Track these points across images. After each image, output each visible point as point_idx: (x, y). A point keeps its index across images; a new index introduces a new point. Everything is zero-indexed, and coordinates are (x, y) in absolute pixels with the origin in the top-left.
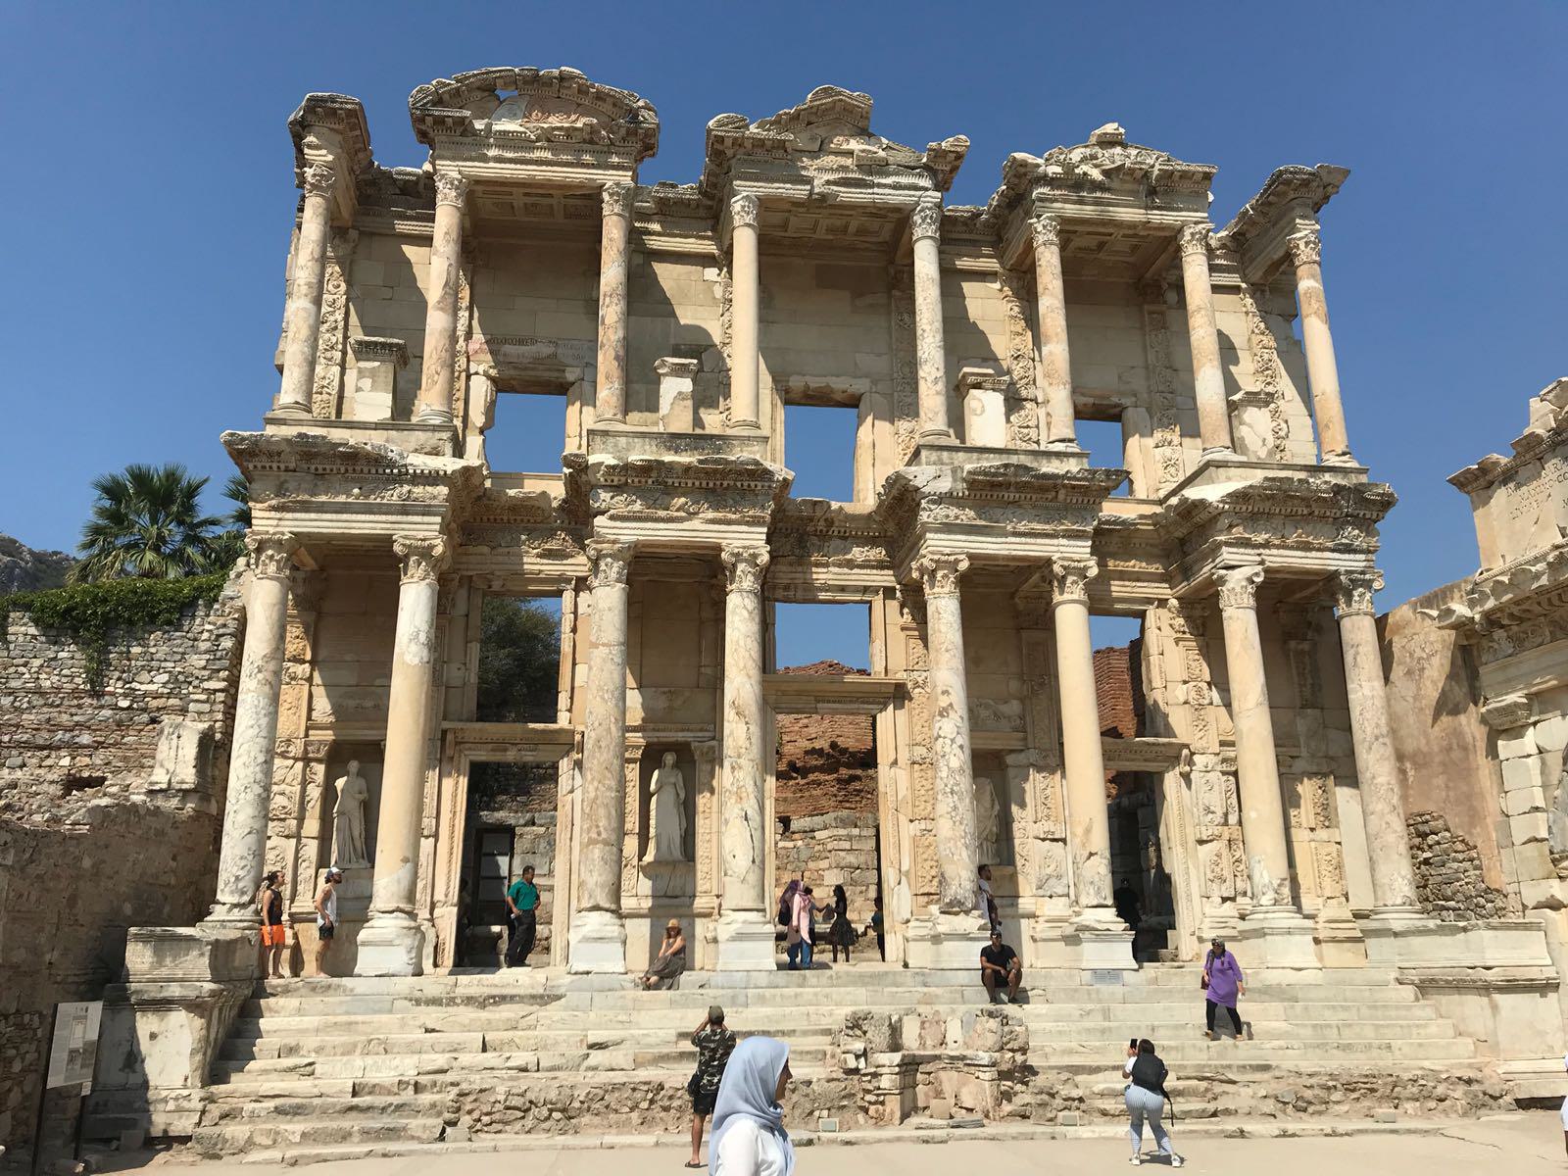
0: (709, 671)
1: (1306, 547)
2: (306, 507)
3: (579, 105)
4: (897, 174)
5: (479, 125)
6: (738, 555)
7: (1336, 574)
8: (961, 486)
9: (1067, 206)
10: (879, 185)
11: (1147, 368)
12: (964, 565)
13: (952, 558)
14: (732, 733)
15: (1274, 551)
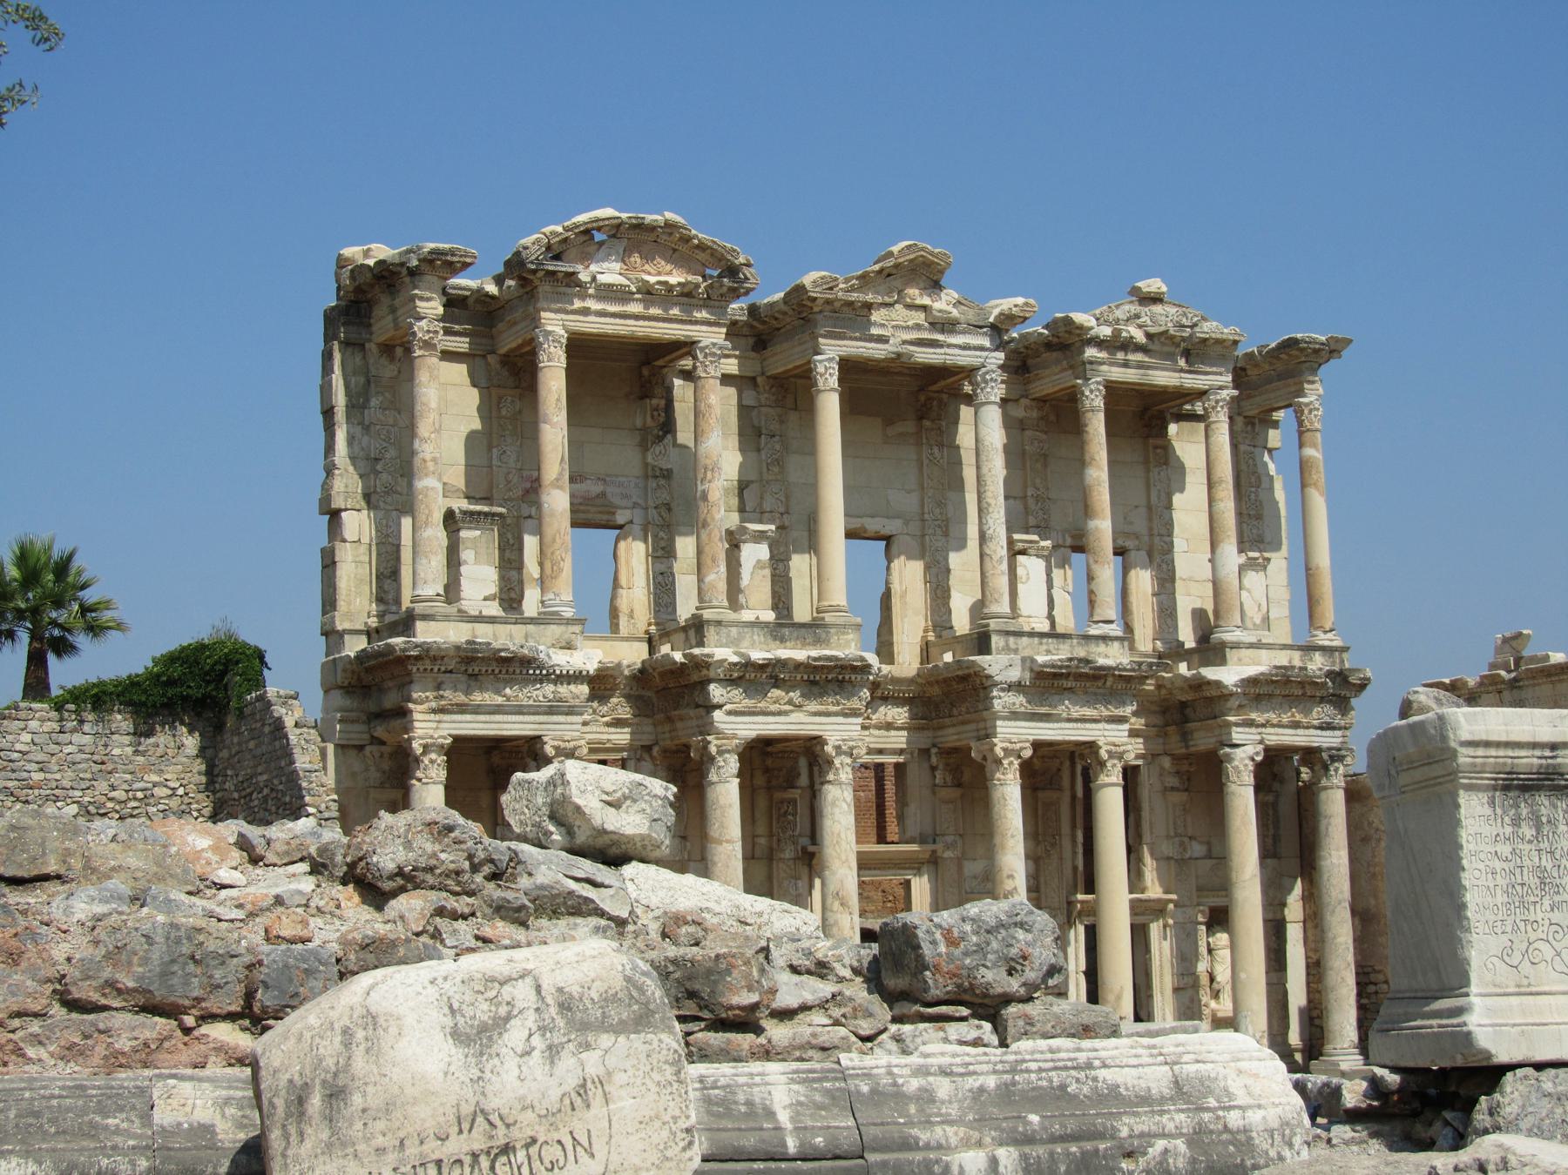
0: (762, 841)
1: (1296, 725)
2: (462, 709)
3: (675, 250)
4: (963, 332)
5: (584, 277)
6: (838, 748)
7: (1318, 750)
8: (1027, 675)
9: (1114, 369)
10: (949, 346)
11: (1149, 508)
12: (1028, 753)
13: (1018, 746)
14: (836, 922)
15: (1272, 730)
